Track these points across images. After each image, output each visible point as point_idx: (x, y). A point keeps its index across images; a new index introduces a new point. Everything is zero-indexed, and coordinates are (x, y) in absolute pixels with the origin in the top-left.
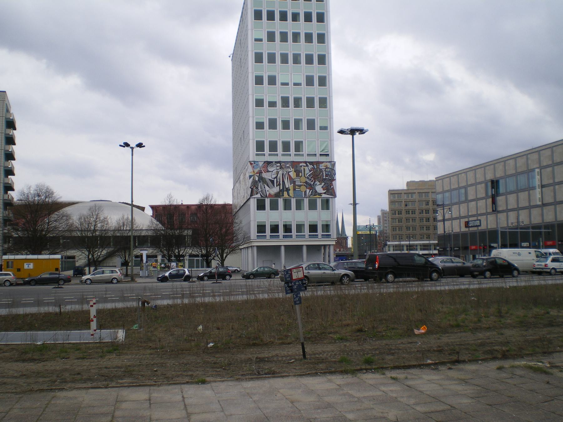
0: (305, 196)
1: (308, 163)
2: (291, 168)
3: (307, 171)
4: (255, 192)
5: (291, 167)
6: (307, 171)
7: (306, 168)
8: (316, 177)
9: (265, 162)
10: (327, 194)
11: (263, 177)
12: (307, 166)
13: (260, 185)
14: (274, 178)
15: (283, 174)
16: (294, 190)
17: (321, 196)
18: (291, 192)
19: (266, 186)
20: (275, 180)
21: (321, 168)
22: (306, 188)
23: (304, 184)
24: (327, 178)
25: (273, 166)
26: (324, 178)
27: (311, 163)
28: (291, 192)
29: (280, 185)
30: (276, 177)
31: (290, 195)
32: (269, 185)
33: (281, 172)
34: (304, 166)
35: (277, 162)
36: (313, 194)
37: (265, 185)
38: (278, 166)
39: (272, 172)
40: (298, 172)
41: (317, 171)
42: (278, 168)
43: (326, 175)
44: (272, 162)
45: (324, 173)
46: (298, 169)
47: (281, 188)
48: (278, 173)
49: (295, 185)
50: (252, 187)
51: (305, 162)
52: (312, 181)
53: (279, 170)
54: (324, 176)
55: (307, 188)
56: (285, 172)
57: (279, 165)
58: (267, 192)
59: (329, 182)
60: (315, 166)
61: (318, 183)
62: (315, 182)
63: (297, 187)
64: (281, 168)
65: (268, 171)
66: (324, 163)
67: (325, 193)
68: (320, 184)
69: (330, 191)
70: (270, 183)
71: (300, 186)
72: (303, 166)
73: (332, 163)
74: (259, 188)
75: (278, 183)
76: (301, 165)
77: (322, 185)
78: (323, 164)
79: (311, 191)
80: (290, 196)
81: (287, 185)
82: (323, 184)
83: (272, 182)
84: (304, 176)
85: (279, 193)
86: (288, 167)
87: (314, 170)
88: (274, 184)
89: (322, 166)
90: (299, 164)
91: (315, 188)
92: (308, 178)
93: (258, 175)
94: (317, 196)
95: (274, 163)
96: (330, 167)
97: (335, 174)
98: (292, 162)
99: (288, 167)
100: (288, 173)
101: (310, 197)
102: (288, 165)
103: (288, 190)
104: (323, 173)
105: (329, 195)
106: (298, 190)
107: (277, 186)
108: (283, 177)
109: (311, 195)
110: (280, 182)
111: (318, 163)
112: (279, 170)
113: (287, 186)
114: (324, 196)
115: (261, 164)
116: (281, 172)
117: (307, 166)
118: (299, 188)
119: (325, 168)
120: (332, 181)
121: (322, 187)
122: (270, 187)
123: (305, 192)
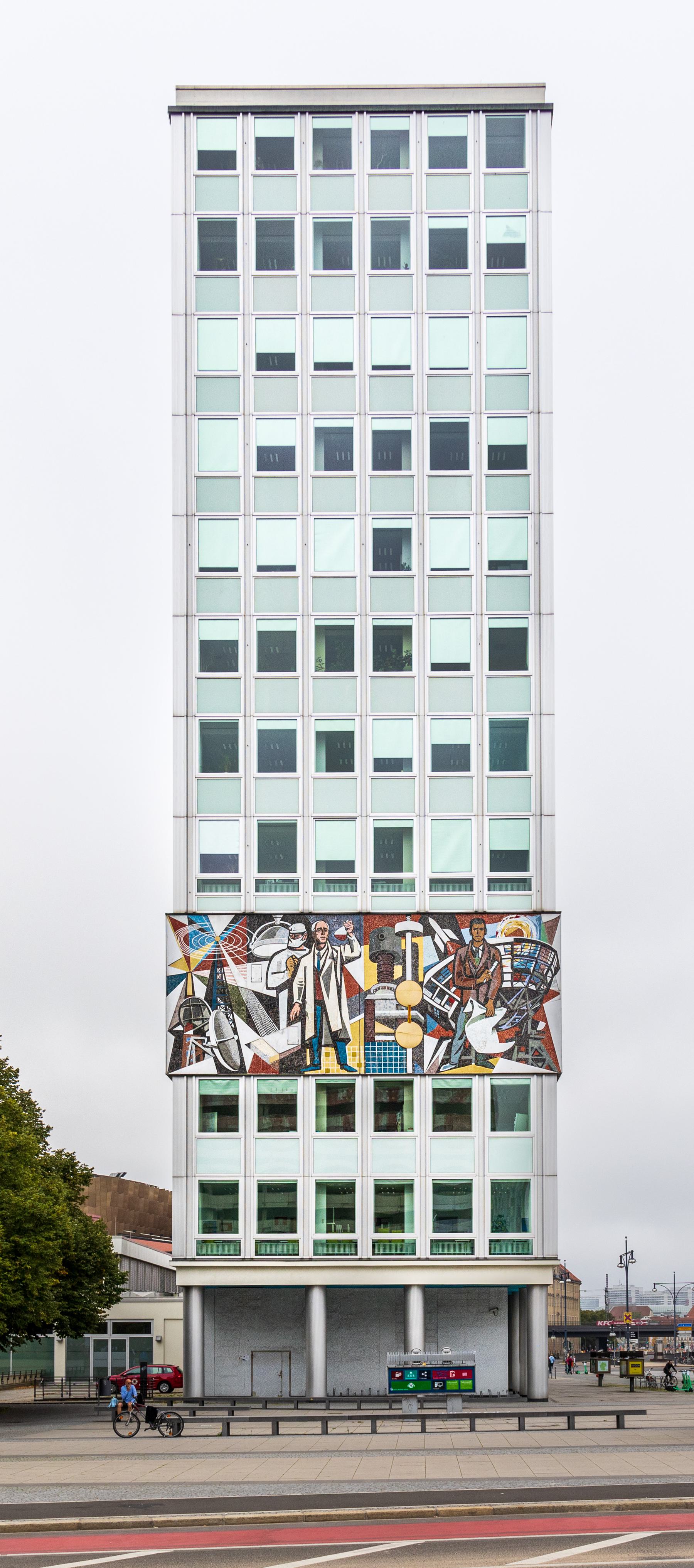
0: (418, 1069)
1: (432, 922)
2: (356, 944)
3: (428, 955)
4: (191, 1052)
5: (353, 938)
6: (428, 955)
7: (425, 943)
8: (470, 983)
9: (237, 917)
10: (519, 1060)
11: (230, 981)
12: (429, 931)
13: (214, 1017)
14: (279, 989)
15: (317, 972)
16: (369, 1039)
17: (493, 1067)
18: (355, 1052)
19: (240, 1023)
20: (284, 996)
21: (491, 941)
22: (420, 1030)
23: (414, 1013)
24: (520, 985)
25: (272, 935)
26: (505, 985)
27: (449, 920)
28: (355, 1052)
29: (302, 1017)
31: (351, 1062)
32: (254, 1017)
33: (308, 963)
34: (415, 934)
35: (290, 918)
36: (455, 1059)
38: (295, 936)
39: (270, 959)
41: (474, 954)
42: (297, 943)
43: (517, 974)
44: (269, 917)
45: (507, 963)
46: (387, 945)
47: (310, 1033)
48: (295, 965)
49: (370, 1019)
50: (180, 1028)
51: (422, 917)
52: (451, 1001)
53: (298, 954)
54: (507, 977)
55: (425, 1032)
56: (329, 962)
57: (299, 928)
58: (244, 1049)
59: (528, 1006)
60: (465, 932)
61: (478, 1010)
62: (462, 1005)
63: (379, 1028)
64: (311, 941)
65: (252, 958)
67: (508, 1055)
68: (486, 1016)
69: (533, 1044)
70: (259, 1011)
71: (394, 1023)
72: (409, 935)
73: (545, 918)
74: (211, 1033)
75: (296, 1009)
76: (399, 927)
77: (494, 1020)
78: (501, 926)
79: (445, 1043)
80: (350, 1069)
82: (501, 1012)
83: (270, 1005)
84: (415, 978)
85: (299, 1054)
86: (344, 940)
87: (462, 951)
90: (393, 926)
91: (464, 1032)
92: (431, 987)
93: (206, 973)
94: (472, 1068)
95: (278, 921)
96: (535, 938)
97: (558, 969)
100: (342, 964)
101: (438, 1073)
102: (341, 931)
103: (339, 1041)
104: (501, 966)
105: (526, 1061)
107: (290, 1023)
108: (317, 986)
109: (443, 1063)
110: (303, 1006)
111: (480, 918)
112: (298, 954)
113: (336, 1026)
114: (502, 1065)
115: (219, 925)
116: (308, 963)
118: (392, 1031)
119: (511, 939)
120: (542, 1001)
121: (497, 1027)
123: (419, 1049)
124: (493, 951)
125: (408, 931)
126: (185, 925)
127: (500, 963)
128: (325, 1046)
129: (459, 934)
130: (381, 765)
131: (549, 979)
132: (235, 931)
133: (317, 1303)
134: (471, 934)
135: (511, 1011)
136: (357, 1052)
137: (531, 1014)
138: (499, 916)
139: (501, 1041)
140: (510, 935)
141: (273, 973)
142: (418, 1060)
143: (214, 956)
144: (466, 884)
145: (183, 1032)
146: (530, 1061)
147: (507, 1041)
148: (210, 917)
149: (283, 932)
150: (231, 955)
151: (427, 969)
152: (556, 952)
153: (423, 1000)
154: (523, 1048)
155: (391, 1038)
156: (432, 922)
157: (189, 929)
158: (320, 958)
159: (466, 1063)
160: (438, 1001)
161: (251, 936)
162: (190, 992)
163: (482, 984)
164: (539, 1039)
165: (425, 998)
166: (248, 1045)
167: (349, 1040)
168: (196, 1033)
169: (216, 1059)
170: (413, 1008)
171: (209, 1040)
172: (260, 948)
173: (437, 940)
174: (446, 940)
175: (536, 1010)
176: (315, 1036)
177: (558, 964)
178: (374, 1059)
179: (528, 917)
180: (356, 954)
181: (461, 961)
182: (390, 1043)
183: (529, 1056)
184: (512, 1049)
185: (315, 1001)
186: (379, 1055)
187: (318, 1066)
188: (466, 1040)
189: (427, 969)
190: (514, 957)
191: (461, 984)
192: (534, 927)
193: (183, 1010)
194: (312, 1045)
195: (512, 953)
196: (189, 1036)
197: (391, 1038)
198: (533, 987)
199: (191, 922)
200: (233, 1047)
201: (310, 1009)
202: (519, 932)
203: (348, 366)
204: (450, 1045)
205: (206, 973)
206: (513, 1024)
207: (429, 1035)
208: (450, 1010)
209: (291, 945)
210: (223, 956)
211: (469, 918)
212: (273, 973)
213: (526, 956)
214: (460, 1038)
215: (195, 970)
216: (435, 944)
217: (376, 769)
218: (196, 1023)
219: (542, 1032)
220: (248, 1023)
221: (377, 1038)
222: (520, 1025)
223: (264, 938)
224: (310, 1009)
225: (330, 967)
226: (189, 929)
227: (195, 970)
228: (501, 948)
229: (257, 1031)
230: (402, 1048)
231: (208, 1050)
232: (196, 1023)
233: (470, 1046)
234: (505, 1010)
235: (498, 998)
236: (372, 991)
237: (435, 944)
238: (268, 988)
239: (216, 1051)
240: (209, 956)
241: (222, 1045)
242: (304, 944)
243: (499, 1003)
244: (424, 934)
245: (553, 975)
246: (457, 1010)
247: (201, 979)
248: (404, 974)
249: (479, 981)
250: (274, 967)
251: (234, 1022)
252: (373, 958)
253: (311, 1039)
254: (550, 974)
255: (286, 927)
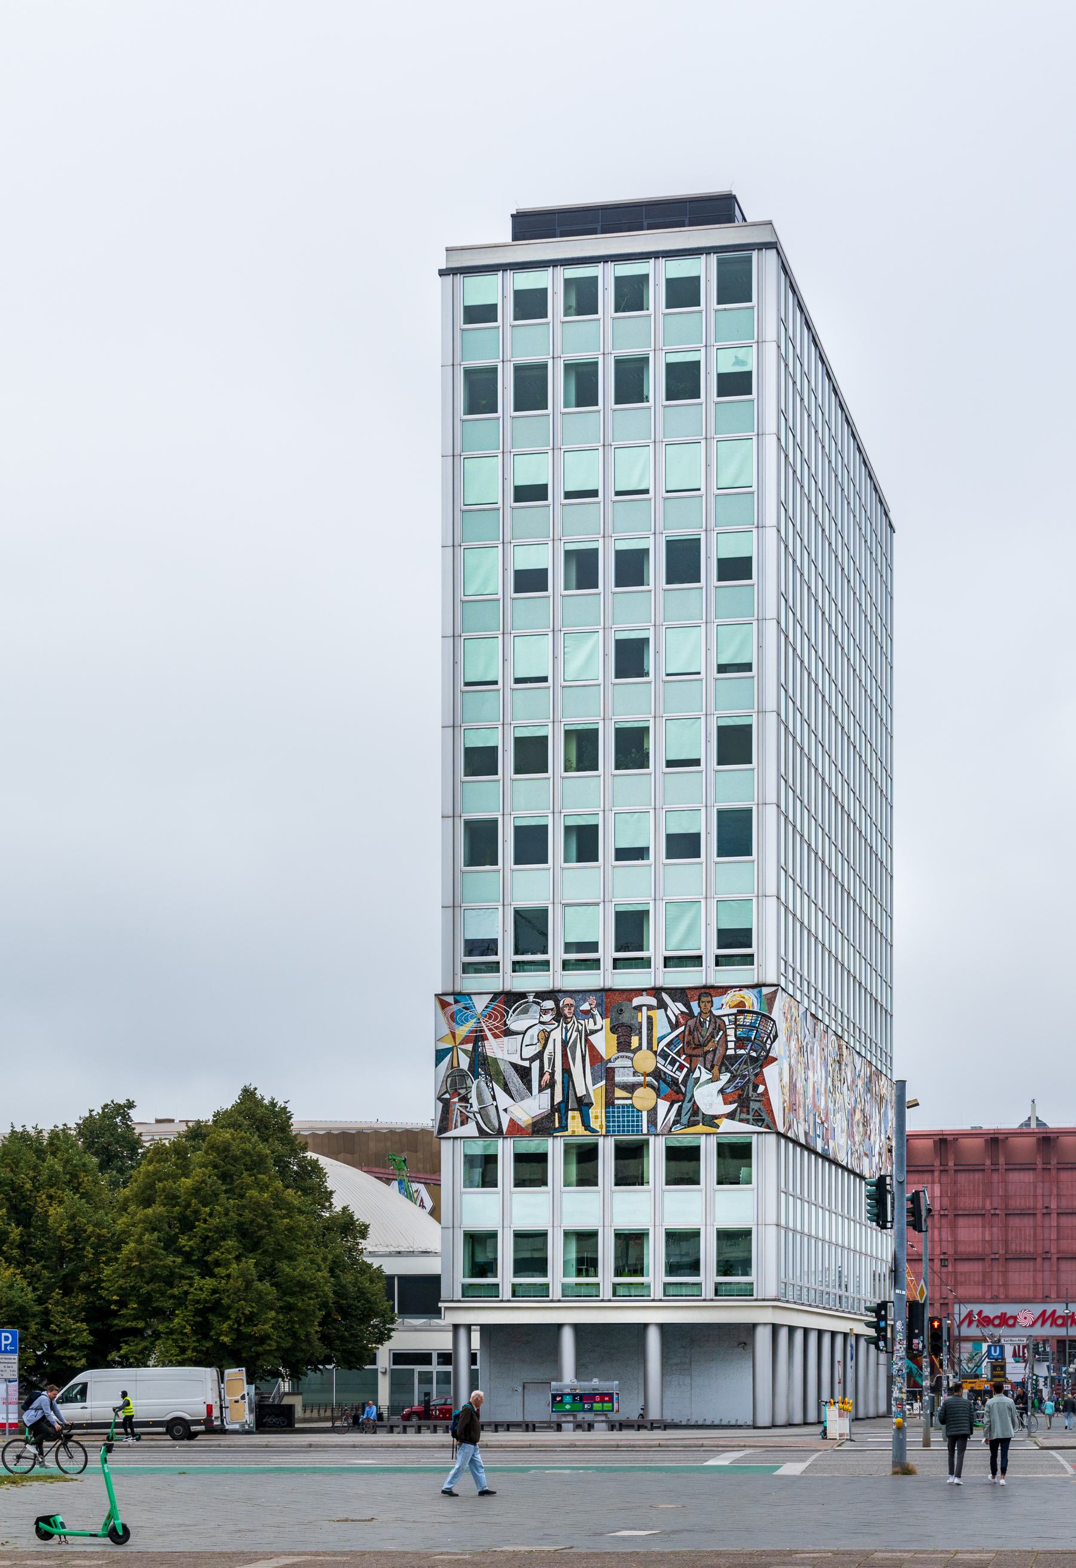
0: (652, 1129)
1: (666, 997)
2: (598, 1018)
3: (661, 1027)
4: (456, 1117)
5: (596, 1012)
6: (661, 1027)
7: (659, 1015)
9: (496, 996)
10: (741, 1120)
11: (489, 1054)
12: (662, 1005)
13: (476, 1086)
14: (532, 1059)
15: (565, 1043)
16: (609, 1103)
17: (718, 1127)
18: (597, 1114)
19: (499, 1091)
20: (536, 1065)
21: (717, 1013)
22: (653, 1094)
23: (649, 1079)
24: (742, 1052)
25: (525, 1011)
26: (730, 1052)
27: (680, 994)
28: (597, 1114)
29: (551, 1085)
30: (539, 1056)
31: (594, 1124)
32: (510, 1085)
33: (557, 1035)
34: (650, 1008)
35: (541, 995)
36: (684, 1119)
37: (496, 1087)
38: (545, 1012)
39: (524, 1033)
40: (624, 1032)
41: (702, 1024)
42: (547, 1018)
43: (740, 1042)
44: (523, 995)
45: (731, 1032)
46: (625, 1018)
47: (558, 1098)
48: (546, 1037)
49: (611, 1085)
50: (447, 1096)
51: (656, 991)
53: (548, 1028)
54: (731, 1045)
55: (658, 1096)
56: (575, 1034)
57: (549, 1004)
58: (501, 1113)
59: (749, 1071)
60: (694, 1005)
61: (705, 1076)
62: (691, 1071)
63: (619, 1093)
64: (559, 1016)
65: (508, 1033)
66: (731, 993)
67: (731, 1116)
68: (712, 1080)
69: (754, 1106)
70: (514, 1080)
71: (631, 1088)
72: (644, 1009)
74: (474, 1100)
75: (547, 1077)
76: (636, 1001)
78: (727, 999)
79: (676, 1106)
80: (593, 1131)
81: (584, 1083)
82: (725, 1077)
83: (524, 1073)
84: (650, 1047)
85: (549, 1117)
86: (587, 1014)
87: (691, 1022)
88: (530, 1081)
89: (723, 1006)
90: (631, 1001)
91: (693, 1096)
92: (664, 1055)
93: (469, 1047)
94: (700, 1128)
95: (531, 998)
96: (756, 1009)
98: (603, 990)
99: (587, 1014)
100: (586, 1035)
102: (586, 1007)
103: (583, 1105)
104: (726, 1035)
105: (747, 1121)
106: (623, 1106)
107: (541, 1090)
108: (564, 1055)
109: (675, 1123)
110: (552, 1074)
111: (709, 991)
112: (548, 1028)
113: (581, 1091)
114: (726, 1125)
115: (480, 1003)
116: (557, 1035)
117: (662, 1005)
119: (735, 1011)
120: (762, 1067)
121: (722, 1091)
122: (514, 1093)
123: (653, 1112)
124: (718, 1021)
125: (644, 1005)
126: (451, 1004)
127: (725, 1032)
128: (571, 1110)
129: (689, 1007)
130: (623, 854)
131: (768, 1046)
132: (494, 1009)
133: (568, 1339)
134: (699, 1006)
135: (734, 1076)
136: (599, 1115)
137: (752, 1078)
138: (724, 990)
139: (725, 1104)
140: (733, 1007)
141: (526, 1046)
142: (652, 1121)
143: (476, 1031)
144: (697, 960)
145: (450, 1099)
146: (751, 1120)
147: (731, 1103)
148: (472, 996)
149: (535, 1007)
150: (490, 1030)
151: (660, 1039)
152: (774, 1021)
153: (657, 1067)
154: (745, 1110)
155: (629, 1102)
156: (666, 997)
157: (455, 1008)
158: (567, 1031)
159: (695, 1123)
160: (670, 1067)
161: (508, 1012)
162: (455, 1064)
163: (709, 1052)
164: (759, 1101)
165: (659, 1065)
166: (505, 1110)
167: (592, 1104)
168: (460, 1100)
169: (477, 1123)
170: (648, 1075)
171: (471, 1107)
172: (516, 1023)
173: (669, 1012)
174: (677, 1012)
175: (756, 1075)
176: (562, 1102)
177: (776, 1032)
178: (614, 1121)
179: (750, 990)
180: (598, 1027)
181: (690, 1031)
182: (628, 1106)
183: (750, 1117)
184: (735, 1111)
185: (563, 1069)
186: (618, 1117)
187: (564, 1128)
188: (695, 1102)
189: (660, 1039)
190: (737, 1026)
191: (690, 1052)
192: (755, 999)
193: (449, 1079)
194: (559, 1110)
195: (735, 1023)
196: (455, 1103)
197: (629, 1102)
198: (754, 1054)
199: (456, 1002)
200: (492, 1111)
201: (558, 1077)
202: (741, 1004)
203: (594, 493)
204: (680, 1108)
205: (469, 1047)
206: (735, 1087)
207: (662, 1099)
208: (681, 1076)
209: (542, 1020)
210: (482, 1031)
211: (697, 993)
212: (526, 1046)
213: (747, 1026)
214: (690, 1101)
215: (460, 1044)
216: (667, 1016)
217: (617, 859)
218: (461, 1091)
219: (762, 1094)
220: (505, 1091)
221: (617, 1102)
222: (742, 1088)
223: (518, 1014)
224: (558, 1077)
225: (576, 1039)
226: (455, 1008)
227: (460, 1044)
228: (726, 1019)
229: (512, 1097)
230: (638, 1111)
231: (471, 1115)
232: (461, 1091)
233: (698, 1108)
234: (729, 1075)
235: (723, 1064)
236: (612, 1060)
237: (667, 1016)
238: (522, 1059)
239: (478, 1116)
240: (472, 1032)
241: (483, 1111)
242: (553, 1019)
243: (723, 1068)
244: (659, 1008)
245: (772, 1043)
246: (687, 1076)
247: (465, 1051)
248: (640, 1044)
249: (706, 1049)
250: (527, 1041)
251: (493, 1090)
252: (613, 1029)
253: (559, 1103)
254: (769, 1042)
255: (538, 1004)
